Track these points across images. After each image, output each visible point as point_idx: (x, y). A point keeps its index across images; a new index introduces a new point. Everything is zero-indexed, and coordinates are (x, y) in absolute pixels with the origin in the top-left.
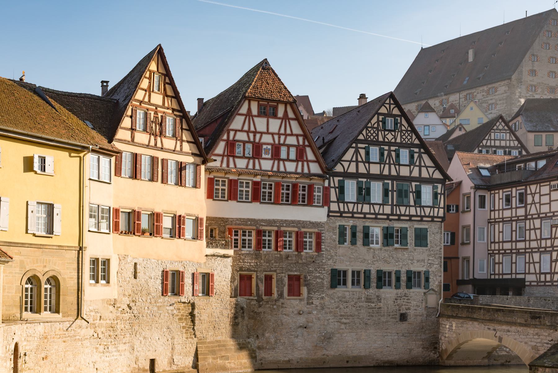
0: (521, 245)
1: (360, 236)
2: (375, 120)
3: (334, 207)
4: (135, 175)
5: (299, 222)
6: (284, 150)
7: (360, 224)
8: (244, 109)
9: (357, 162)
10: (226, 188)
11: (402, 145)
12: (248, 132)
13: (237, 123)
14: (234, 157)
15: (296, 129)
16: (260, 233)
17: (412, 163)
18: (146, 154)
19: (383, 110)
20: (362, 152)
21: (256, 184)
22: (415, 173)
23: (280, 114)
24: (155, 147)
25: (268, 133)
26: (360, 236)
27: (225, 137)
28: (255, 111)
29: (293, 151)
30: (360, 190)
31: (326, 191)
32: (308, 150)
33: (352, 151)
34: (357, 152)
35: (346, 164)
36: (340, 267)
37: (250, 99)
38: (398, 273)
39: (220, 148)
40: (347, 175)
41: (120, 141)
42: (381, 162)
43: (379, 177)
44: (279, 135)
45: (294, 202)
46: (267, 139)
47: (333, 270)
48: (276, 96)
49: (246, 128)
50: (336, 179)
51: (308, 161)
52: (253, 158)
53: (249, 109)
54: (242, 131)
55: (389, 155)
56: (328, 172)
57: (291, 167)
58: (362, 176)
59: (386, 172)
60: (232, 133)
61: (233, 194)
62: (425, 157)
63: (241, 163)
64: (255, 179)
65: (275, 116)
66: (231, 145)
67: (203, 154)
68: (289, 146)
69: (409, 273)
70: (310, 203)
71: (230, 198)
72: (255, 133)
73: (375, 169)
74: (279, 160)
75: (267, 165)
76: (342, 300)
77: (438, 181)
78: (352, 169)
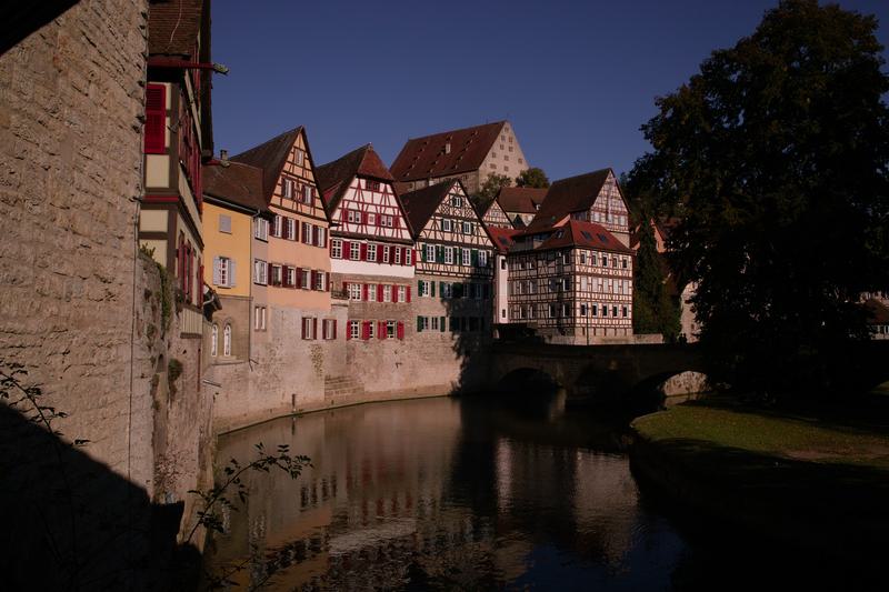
0: (533, 298)
1: (437, 289)
2: (447, 198)
3: (419, 266)
4: (285, 236)
5: (394, 278)
6: (384, 219)
7: (437, 281)
8: (355, 182)
9: (435, 231)
10: (341, 248)
11: (465, 219)
12: (358, 202)
13: (350, 194)
14: (347, 222)
15: (394, 202)
16: (366, 287)
17: (473, 233)
18: (293, 217)
19: (452, 191)
20: (439, 223)
21: (364, 246)
22: (475, 242)
23: (382, 189)
24: (296, 212)
25: (372, 204)
26: (437, 289)
27: (341, 206)
28: (363, 186)
29: (391, 220)
30: (437, 252)
31: (414, 252)
32: (401, 219)
33: (431, 222)
34: (435, 223)
35: (428, 232)
36: (423, 315)
37: (359, 177)
38: (464, 319)
39: (337, 215)
40: (428, 240)
41: (273, 205)
42: (452, 231)
43: (451, 243)
44: (381, 206)
45: (392, 262)
46: (372, 209)
47: (419, 317)
48: (380, 175)
49: (356, 199)
50: (421, 244)
51: (401, 229)
52: (362, 224)
53: (359, 184)
54: (353, 201)
55: (457, 226)
56: (416, 238)
57: (389, 233)
58: (439, 242)
59: (455, 240)
60: (346, 203)
61: (347, 255)
62: (481, 228)
63: (353, 228)
64: (363, 242)
65: (378, 192)
66: (345, 213)
67: (329, 219)
68: (388, 215)
69: (471, 318)
70: (403, 264)
71: (344, 258)
72: (363, 203)
73: (448, 237)
74: (381, 226)
75: (371, 230)
76: (425, 341)
77: (489, 248)
78: (432, 237)
